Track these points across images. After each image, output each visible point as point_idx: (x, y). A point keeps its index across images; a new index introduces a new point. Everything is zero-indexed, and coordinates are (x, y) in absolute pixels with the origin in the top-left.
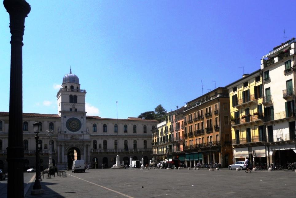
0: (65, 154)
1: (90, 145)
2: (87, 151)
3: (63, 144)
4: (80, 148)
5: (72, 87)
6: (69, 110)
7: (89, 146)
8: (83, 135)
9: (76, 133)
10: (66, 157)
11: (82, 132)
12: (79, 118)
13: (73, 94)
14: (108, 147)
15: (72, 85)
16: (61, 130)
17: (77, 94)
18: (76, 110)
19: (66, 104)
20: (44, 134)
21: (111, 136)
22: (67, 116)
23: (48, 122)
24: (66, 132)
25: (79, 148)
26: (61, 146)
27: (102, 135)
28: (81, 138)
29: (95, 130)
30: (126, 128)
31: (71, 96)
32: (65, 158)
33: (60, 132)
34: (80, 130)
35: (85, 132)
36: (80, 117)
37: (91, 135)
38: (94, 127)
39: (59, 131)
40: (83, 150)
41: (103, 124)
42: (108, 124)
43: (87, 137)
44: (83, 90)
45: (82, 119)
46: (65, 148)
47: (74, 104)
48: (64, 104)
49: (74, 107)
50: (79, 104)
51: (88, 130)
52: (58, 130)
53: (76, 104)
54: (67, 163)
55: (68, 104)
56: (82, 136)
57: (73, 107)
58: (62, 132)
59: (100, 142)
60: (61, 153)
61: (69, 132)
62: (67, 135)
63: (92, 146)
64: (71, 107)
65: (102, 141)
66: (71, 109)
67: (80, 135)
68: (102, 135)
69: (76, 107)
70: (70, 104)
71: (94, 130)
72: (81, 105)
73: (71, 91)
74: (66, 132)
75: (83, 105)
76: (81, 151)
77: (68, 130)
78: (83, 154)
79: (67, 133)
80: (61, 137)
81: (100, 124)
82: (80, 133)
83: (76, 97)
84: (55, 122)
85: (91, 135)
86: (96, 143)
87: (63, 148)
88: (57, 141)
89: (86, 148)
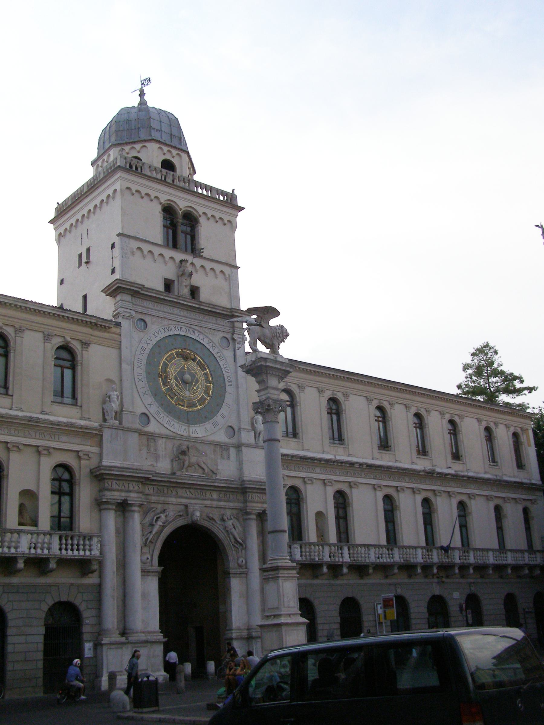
0: (145, 572)
3: (133, 497)
8: (239, 447)
9: (198, 431)
11: (232, 430)
18: (194, 291)
19: (146, 248)
22: (148, 319)
23: (47, 337)
24: (146, 417)
25: (221, 535)
26: (123, 507)
28: (227, 470)
32: (144, 595)
33: (118, 415)
36: (217, 337)
39: (115, 406)
40: (241, 545)
48: (135, 244)
50: (208, 265)
54: (160, 637)
60: (123, 564)
61: (162, 423)
62: (151, 437)
64: (170, 272)
66: (168, 285)
67: (223, 447)
69: (197, 280)
70: (169, 253)
72: (218, 268)
74: (146, 417)
76: (231, 553)
78: (245, 573)
80: (120, 453)
82: (222, 437)
84: (85, 344)
87: (136, 520)
88: (99, 476)
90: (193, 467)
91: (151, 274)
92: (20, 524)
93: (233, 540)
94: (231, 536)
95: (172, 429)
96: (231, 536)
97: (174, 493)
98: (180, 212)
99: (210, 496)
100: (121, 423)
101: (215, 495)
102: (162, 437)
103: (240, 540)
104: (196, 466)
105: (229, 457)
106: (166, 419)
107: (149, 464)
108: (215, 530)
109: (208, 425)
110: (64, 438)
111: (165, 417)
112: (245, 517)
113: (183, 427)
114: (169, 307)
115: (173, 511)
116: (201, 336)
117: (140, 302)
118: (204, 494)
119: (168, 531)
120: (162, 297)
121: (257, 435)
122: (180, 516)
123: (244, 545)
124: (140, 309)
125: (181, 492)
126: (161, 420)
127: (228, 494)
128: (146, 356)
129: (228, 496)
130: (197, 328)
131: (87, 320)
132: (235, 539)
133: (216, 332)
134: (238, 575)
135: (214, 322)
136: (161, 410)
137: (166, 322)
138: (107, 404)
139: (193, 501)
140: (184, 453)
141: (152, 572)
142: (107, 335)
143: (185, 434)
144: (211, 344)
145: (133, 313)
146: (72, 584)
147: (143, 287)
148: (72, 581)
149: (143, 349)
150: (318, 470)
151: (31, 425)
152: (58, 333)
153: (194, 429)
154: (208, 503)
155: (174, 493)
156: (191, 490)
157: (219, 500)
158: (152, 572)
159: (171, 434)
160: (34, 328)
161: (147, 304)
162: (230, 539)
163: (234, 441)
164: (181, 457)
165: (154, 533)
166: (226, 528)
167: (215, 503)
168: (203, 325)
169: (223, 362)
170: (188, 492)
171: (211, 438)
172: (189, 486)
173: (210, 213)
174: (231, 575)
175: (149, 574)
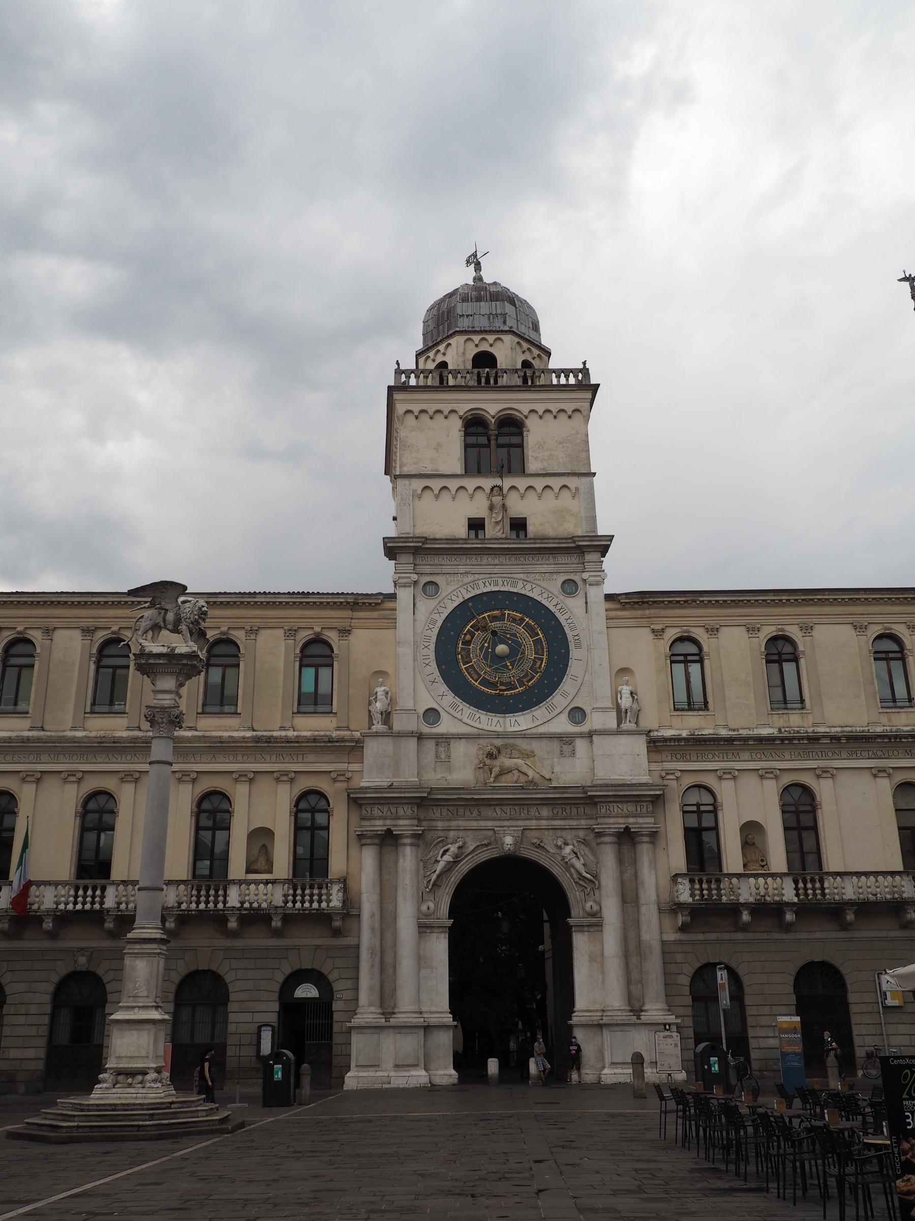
0: (424, 928)
1: (654, 836)
2: (629, 898)
4: (568, 866)
5: (484, 360)
6: (461, 531)
7: (644, 851)
9: (521, 722)
10: (439, 947)
11: (577, 714)
12: (540, 584)
13: (492, 405)
14: (833, 858)
15: (484, 347)
16: (392, 702)
17: (522, 404)
18: (519, 525)
20: (249, 734)
21: (856, 742)
22: (438, 579)
25: (556, 871)
27: (760, 740)
28: (572, 771)
29: (698, 697)
30: (896, 666)
31: (474, 424)
32: (421, 961)
34: (560, 700)
35: (604, 710)
37: (656, 745)
38: (679, 668)
40: (591, 883)
41: (768, 631)
42: (807, 629)
43: (623, 761)
44: (567, 372)
45: (575, 604)
46: (425, 864)
47: (497, 481)
49: (504, 507)
50: (539, 483)
51: (626, 690)
52: (372, 698)
53: (522, 483)
55: (453, 484)
56: (581, 745)
57: (491, 508)
58: (399, 724)
59: (749, 801)
62: (444, 740)
63: (676, 855)
64: (478, 508)
65: (771, 790)
66: (476, 525)
67: (565, 740)
68: (765, 732)
69: (518, 507)
70: (470, 483)
71: (682, 697)
72: (556, 483)
73: (473, 383)
74: (432, 715)
75: (572, 482)
76: (574, 895)
77: (450, 698)
78: (595, 924)
79: (445, 726)
81: (739, 634)
82: (562, 725)
83: (512, 425)
84: (345, 632)
85: (656, 745)
86: (707, 821)
87: (407, 859)
89: (620, 862)
90: (510, 774)
91: (447, 518)
92: (248, 871)
93: (575, 876)
94: (572, 870)
95: (476, 725)
96: (572, 870)
97: (475, 813)
98: (493, 421)
99: (537, 814)
100: (391, 728)
101: (545, 812)
102: (460, 737)
103: (588, 876)
104: (515, 772)
105: (573, 753)
106: (467, 711)
107: (439, 776)
108: (545, 863)
109: (540, 712)
110: (311, 757)
111: (465, 709)
112: (599, 841)
113: (495, 720)
114: (474, 557)
115: (468, 842)
116: (528, 587)
117: (429, 559)
118: (526, 812)
119: (464, 867)
120: (459, 546)
121: (623, 714)
122: (486, 845)
123: (597, 882)
124: (428, 569)
125: (489, 812)
126: (458, 715)
127: (568, 808)
128: (436, 631)
129: (568, 811)
130: (522, 576)
131: (342, 600)
132: (580, 874)
133: (555, 576)
134: (586, 929)
135: (551, 561)
136: (458, 700)
137: (470, 578)
138: (373, 706)
139: (506, 823)
140: (490, 755)
141: (439, 927)
142: (375, 614)
143: (498, 729)
144: (545, 595)
145: (415, 577)
146: (318, 947)
147: (426, 540)
148: (318, 942)
149: (434, 622)
150: (745, 755)
151: (264, 746)
152: (304, 625)
153: (513, 720)
154: (533, 823)
155: (475, 813)
156: (504, 808)
157: (553, 819)
158: (439, 927)
159: (475, 731)
160: (270, 625)
161: (438, 560)
162: (571, 875)
163: (585, 728)
164: (488, 761)
165: (437, 872)
166: (563, 858)
167: (544, 823)
168: (531, 570)
169: (566, 616)
170: (498, 811)
171: (542, 730)
172: (501, 803)
173: (540, 408)
174: (574, 929)
175: (434, 930)
